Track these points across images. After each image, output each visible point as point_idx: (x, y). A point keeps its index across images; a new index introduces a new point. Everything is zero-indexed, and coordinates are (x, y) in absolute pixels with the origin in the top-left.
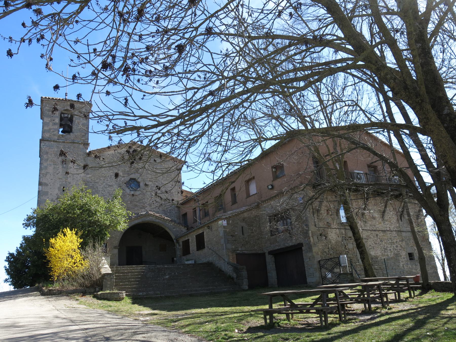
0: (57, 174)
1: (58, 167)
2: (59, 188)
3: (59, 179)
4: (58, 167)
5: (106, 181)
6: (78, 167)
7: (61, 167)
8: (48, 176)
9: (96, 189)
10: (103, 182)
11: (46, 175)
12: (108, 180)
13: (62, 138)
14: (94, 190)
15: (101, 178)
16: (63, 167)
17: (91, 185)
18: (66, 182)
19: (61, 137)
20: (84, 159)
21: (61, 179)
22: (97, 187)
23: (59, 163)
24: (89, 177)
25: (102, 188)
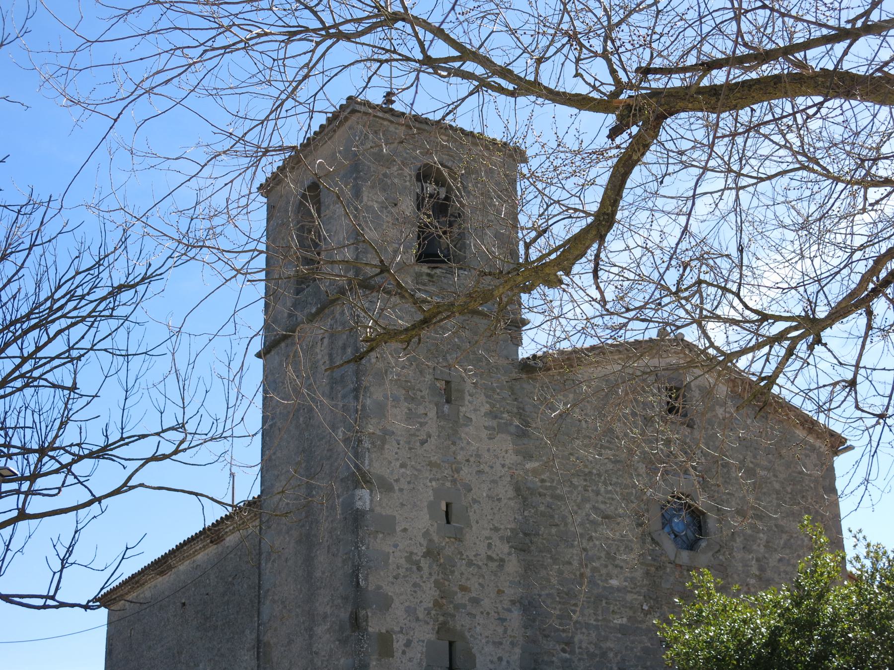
0: (423, 442)
1: (421, 410)
2: (432, 507)
3: (430, 464)
4: (421, 410)
5: (591, 494)
6: (494, 423)
7: (432, 414)
8: (390, 447)
9: (562, 528)
10: (586, 500)
11: (384, 441)
12: (598, 493)
13: (432, 288)
14: (554, 530)
15: (575, 481)
16: (440, 416)
17: (542, 508)
18: (454, 481)
19: (425, 278)
20: (512, 389)
21: (438, 466)
22: (564, 518)
23: (425, 392)
24: (535, 472)
25: (581, 524)
